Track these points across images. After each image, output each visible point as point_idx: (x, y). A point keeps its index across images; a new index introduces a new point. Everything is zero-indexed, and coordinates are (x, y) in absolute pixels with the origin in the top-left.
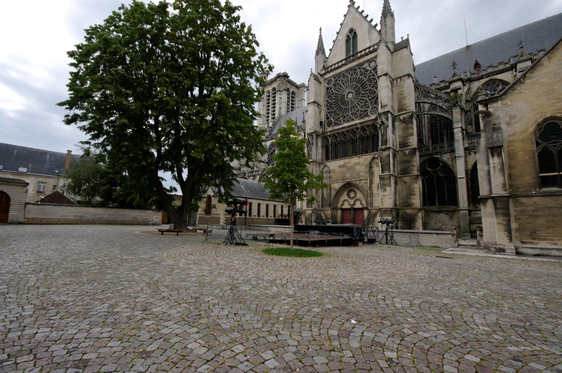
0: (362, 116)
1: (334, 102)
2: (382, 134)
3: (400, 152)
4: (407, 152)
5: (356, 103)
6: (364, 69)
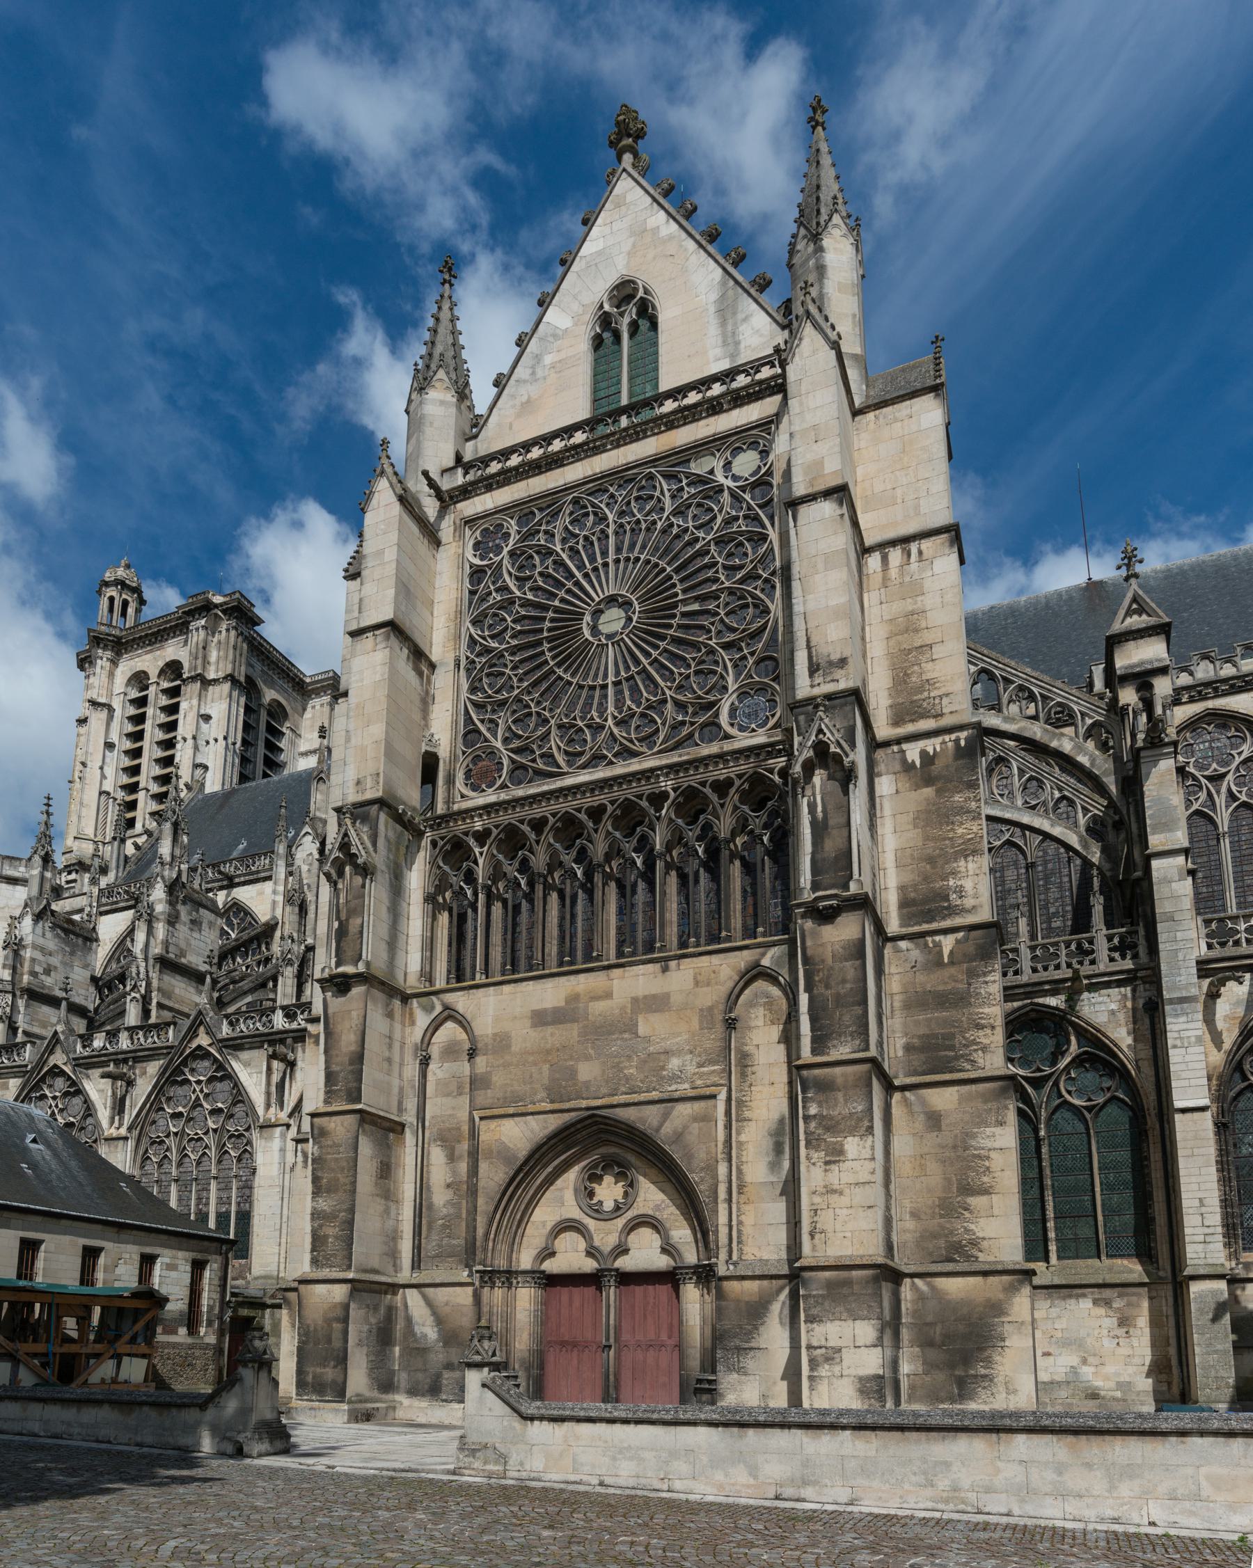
2: (814, 823)
3: (903, 944)
4: (948, 943)
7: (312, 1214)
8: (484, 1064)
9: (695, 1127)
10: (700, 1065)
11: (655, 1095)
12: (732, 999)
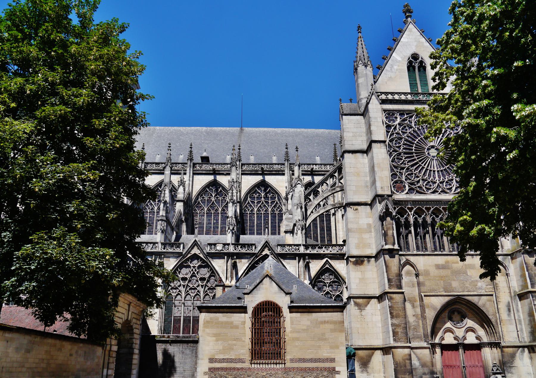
9: (488, 303)
11: (475, 293)
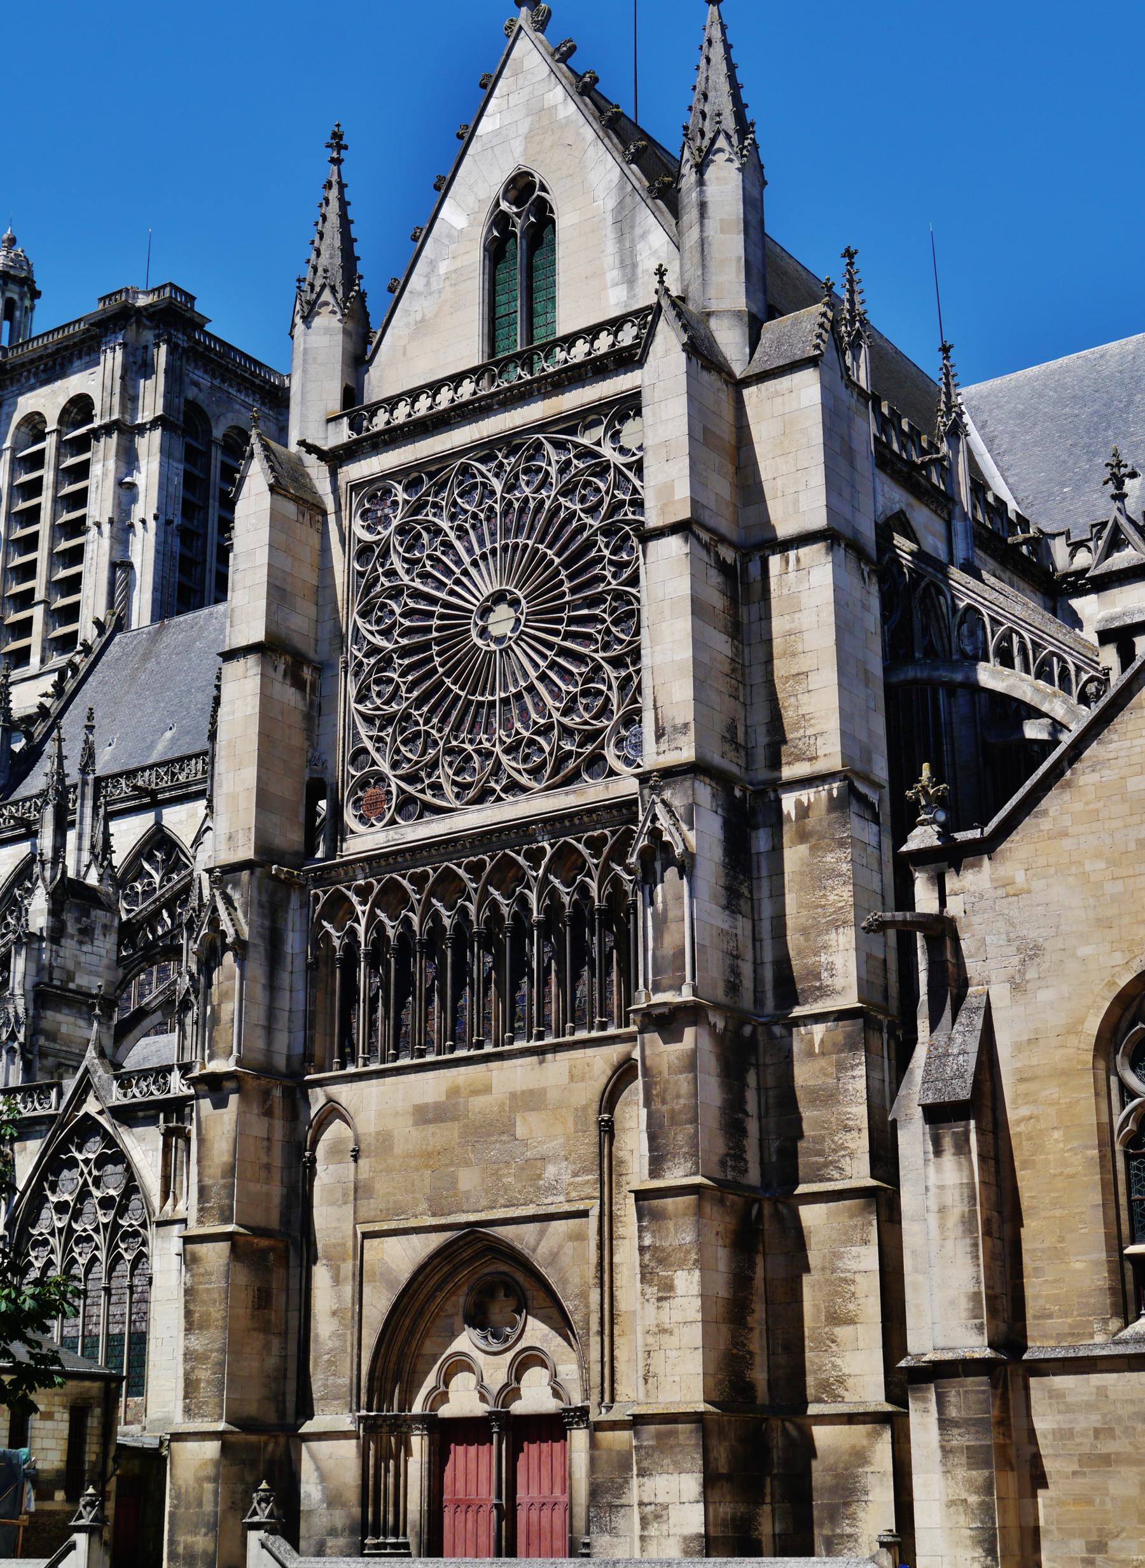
0: (571, 764)
1: (405, 652)
5: (533, 674)
6: (586, 453)
7: (185, 1355)
8: (367, 1167)
9: (569, 1247)
10: (575, 1174)
11: (530, 1210)
12: (610, 1099)
